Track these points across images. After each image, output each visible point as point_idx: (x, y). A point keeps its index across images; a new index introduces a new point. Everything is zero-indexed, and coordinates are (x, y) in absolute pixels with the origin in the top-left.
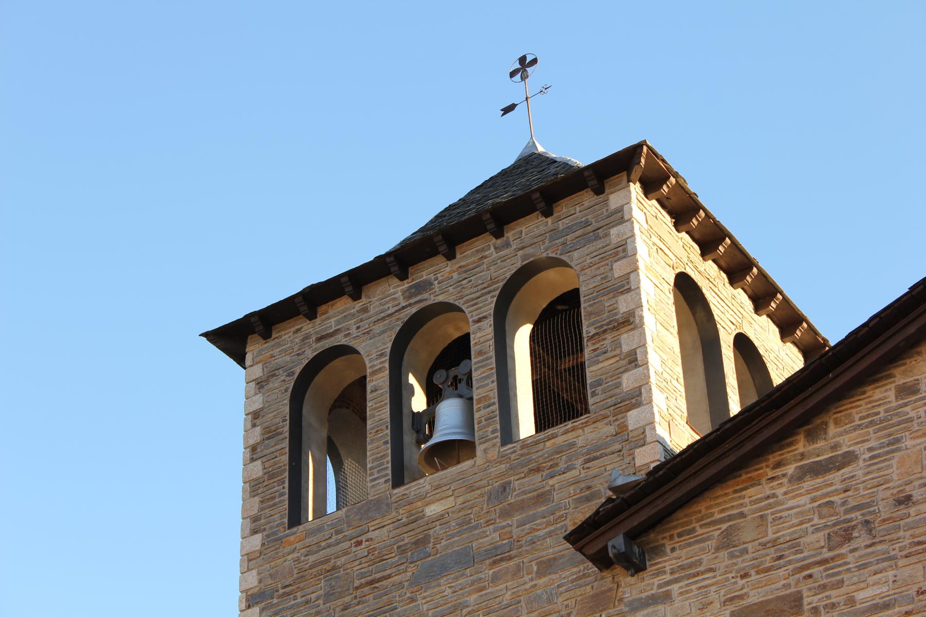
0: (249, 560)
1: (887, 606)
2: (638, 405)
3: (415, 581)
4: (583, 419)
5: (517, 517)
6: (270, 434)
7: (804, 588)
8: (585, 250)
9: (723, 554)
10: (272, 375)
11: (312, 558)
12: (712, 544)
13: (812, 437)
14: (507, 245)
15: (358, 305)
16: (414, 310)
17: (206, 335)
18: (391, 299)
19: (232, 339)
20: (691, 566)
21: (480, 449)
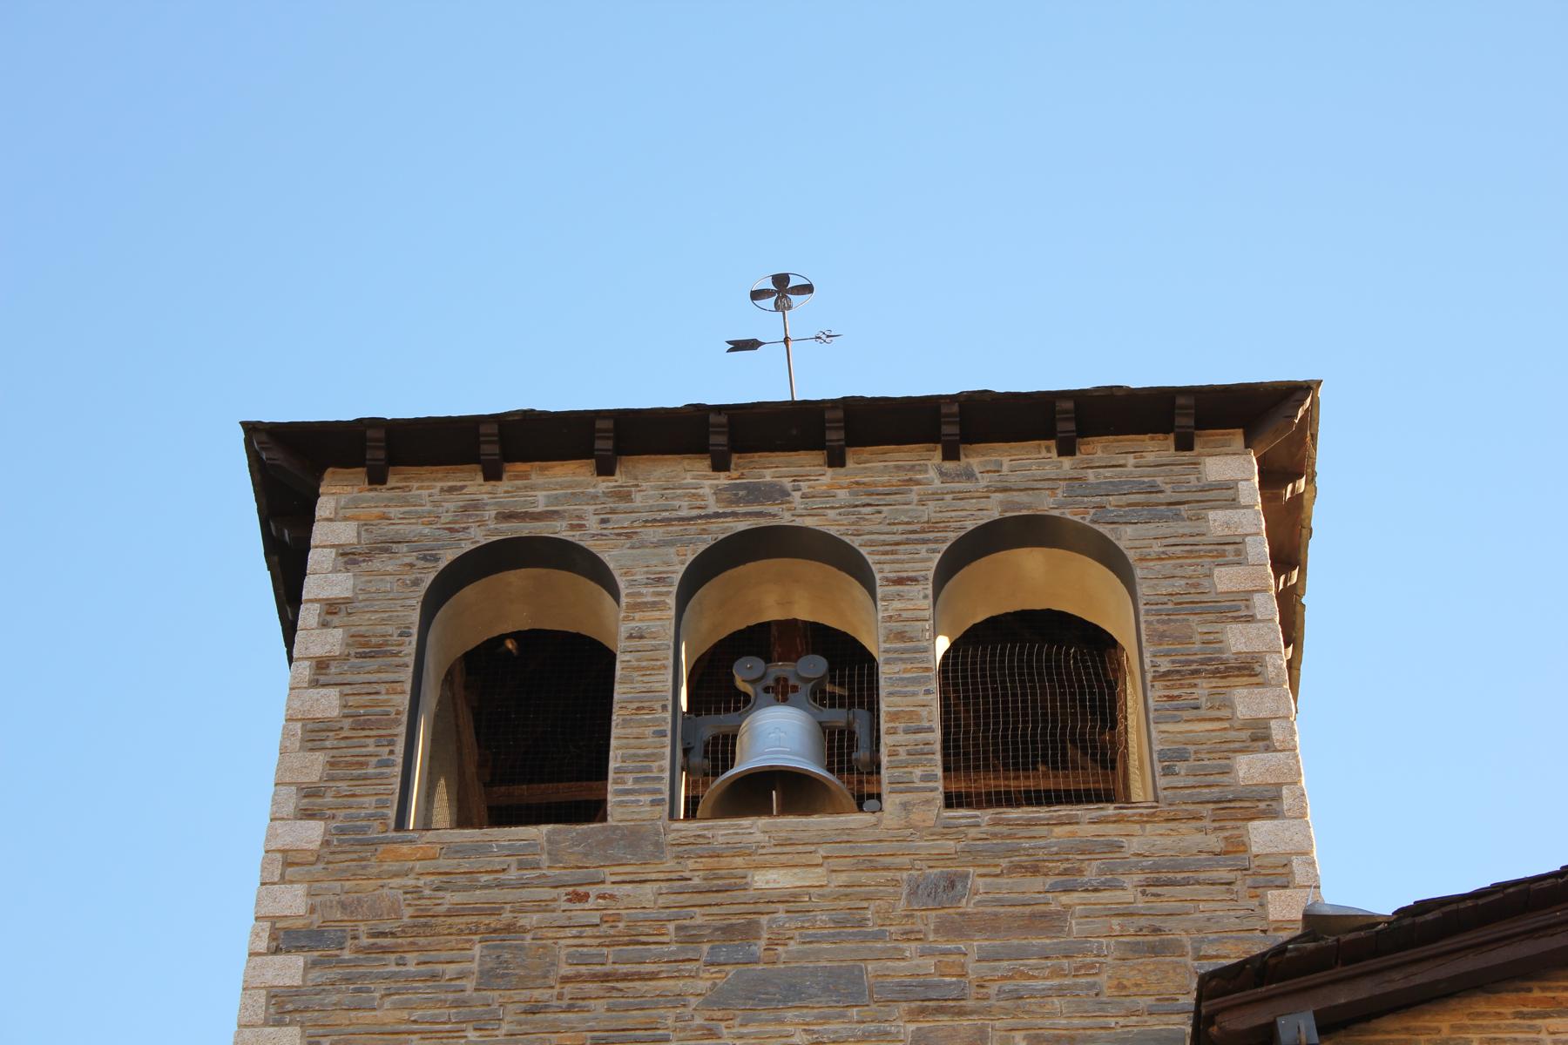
0: (286, 864)
3: (717, 1000)
5: (978, 943)
8: (1152, 529)
11: (451, 898)
15: (604, 485)
16: (742, 526)
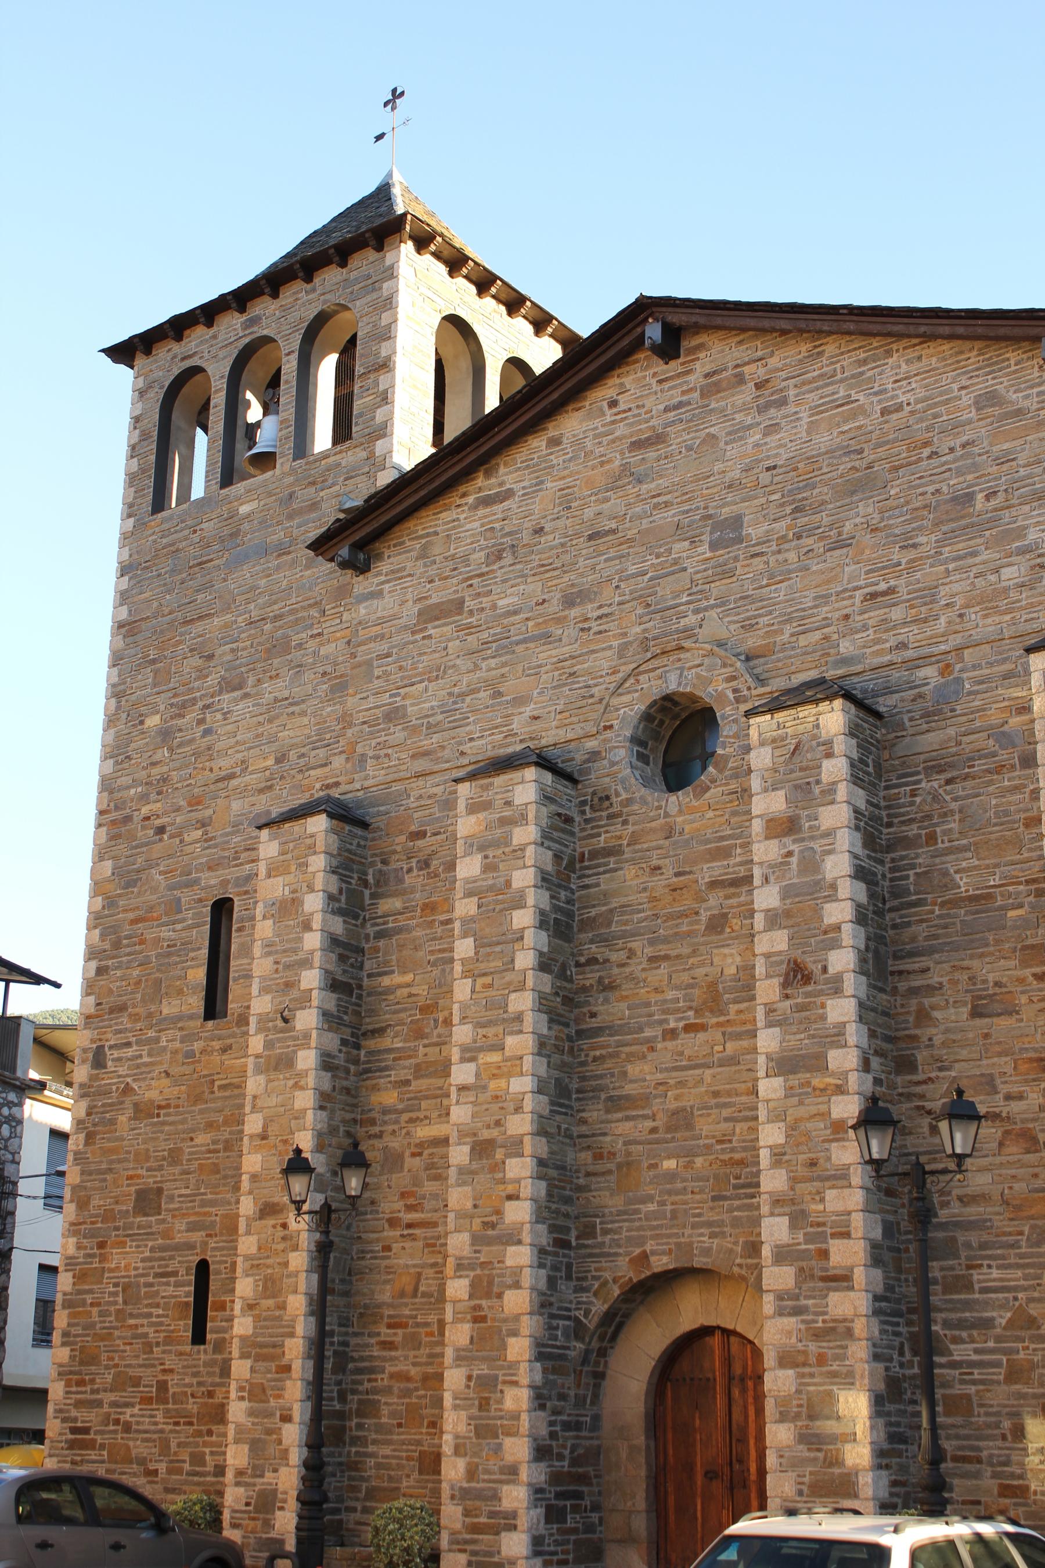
0: (126, 538)
1: (515, 613)
2: (384, 436)
4: (348, 444)
6: (144, 436)
7: (467, 594)
8: (364, 301)
9: (420, 563)
10: (149, 387)
12: (414, 554)
13: (488, 474)
14: (314, 290)
15: (211, 332)
16: (247, 340)
17: (103, 351)
18: (232, 328)
19: (122, 353)
20: (398, 571)
21: (279, 462)
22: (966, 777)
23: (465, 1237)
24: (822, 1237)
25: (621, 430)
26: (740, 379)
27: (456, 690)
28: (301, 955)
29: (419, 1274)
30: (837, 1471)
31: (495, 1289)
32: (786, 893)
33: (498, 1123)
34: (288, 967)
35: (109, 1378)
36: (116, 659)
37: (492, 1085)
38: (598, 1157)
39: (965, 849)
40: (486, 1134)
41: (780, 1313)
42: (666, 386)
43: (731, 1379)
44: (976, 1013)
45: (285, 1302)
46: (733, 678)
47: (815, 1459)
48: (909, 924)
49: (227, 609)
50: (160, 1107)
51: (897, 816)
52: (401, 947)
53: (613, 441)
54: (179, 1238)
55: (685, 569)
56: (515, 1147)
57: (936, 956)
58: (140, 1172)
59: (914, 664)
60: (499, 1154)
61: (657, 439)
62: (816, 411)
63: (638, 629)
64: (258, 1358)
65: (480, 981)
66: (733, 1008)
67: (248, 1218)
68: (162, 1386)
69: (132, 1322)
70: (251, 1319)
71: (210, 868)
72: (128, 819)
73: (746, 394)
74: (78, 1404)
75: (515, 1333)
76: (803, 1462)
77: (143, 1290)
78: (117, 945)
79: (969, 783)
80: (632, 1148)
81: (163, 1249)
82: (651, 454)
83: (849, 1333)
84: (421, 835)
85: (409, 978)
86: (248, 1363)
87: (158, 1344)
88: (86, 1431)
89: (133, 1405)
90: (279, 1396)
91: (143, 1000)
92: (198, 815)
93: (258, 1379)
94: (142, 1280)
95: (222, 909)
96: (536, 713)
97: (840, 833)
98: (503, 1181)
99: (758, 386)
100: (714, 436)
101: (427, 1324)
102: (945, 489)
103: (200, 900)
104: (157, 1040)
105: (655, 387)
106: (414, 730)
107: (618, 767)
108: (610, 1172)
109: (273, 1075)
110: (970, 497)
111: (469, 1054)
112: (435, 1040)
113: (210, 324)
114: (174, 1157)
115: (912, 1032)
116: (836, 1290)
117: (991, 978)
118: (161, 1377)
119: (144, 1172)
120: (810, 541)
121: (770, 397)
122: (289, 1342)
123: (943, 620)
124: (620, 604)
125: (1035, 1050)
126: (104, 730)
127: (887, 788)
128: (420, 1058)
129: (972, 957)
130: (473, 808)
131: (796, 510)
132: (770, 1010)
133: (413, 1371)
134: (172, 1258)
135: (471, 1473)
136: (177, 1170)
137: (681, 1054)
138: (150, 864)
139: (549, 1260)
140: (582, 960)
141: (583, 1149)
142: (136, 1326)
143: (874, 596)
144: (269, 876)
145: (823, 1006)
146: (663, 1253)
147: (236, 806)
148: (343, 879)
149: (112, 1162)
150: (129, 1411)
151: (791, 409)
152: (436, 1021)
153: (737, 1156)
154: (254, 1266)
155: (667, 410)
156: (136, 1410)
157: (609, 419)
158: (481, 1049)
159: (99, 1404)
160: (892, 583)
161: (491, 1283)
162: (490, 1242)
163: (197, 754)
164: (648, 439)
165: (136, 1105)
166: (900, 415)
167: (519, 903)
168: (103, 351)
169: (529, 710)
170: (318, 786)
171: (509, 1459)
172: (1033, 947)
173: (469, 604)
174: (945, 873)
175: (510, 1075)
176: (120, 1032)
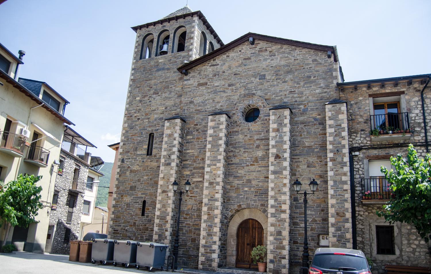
0: (133, 63)
1: (218, 86)
2: (191, 51)
3: (156, 71)
4: (183, 51)
5: (172, 64)
6: (139, 45)
7: (208, 82)
9: (199, 75)
10: (140, 36)
11: (142, 65)
12: (197, 73)
13: (214, 60)
14: (178, 22)
15: (155, 27)
16: (162, 30)
17: (132, 28)
18: (159, 27)
19: (135, 29)
20: (194, 76)
21: (168, 53)
22: (308, 125)
23: (207, 200)
24: (281, 204)
25: (241, 56)
26: (266, 50)
27: (205, 99)
28: (173, 145)
29: (193, 206)
30: (281, 245)
31: (213, 209)
32: (276, 142)
33: (215, 179)
34: (170, 147)
35: (123, 221)
36: (130, 86)
37: (214, 172)
38: (231, 187)
39: (308, 138)
40: (212, 181)
41: (272, 217)
42: (251, 49)
43: (253, 228)
44: (308, 167)
45: (167, 209)
46: (263, 103)
47: (277, 243)
48: (296, 150)
49: (155, 79)
50: (136, 171)
51: (295, 131)
52: (192, 145)
53: (240, 58)
54: (139, 196)
55: (253, 83)
56: (218, 184)
57: (301, 156)
58: (131, 183)
59: (299, 105)
60: (215, 185)
61: (249, 59)
62: (281, 58)
63: (244, 92)
64: (161, 219)
65: (212, 153)
66: (260, 162)
67: (159, 193)
68: (135, 223)
69: (128, 211)
70: (159, 212)
71: (149, 127)
72: (131, 116)
73: (268, 53)
74: (116, 225)
75: (216, 218)
76: (275, 243)
77: (131, 205)
78: (128, 140)
79: (309, 127)
80: (238, 185)
81: (135, 197)
82: (247, 61)
83: (285, 221)
84: (197, 125)
85: (193, 151)
86: (159, 220)
87: (134, 215)
88: (117, 231)
89: (128, 226)
90: (165, 227)
91: (133, 151)
92: (148, 117)
93: (161, 223)
94: (131, 203)
95: (151, 136)
96: (222, 105)
97: (287, 133)
98: (215, 190)
99: (270, 52)
100: (261, 60)
101: (194, 215)
102: (306, 75)
103: (147, 133)
104: (136, 158)
105: (249, 49)
106: (196, 106)
107: (239, 117)
108: (234, 190)
109: (166, 166)
110: (310, 77)
111: (209, 166)
112: (198, 163)
113: (154, 26)
114: (139, 180)
115: (296, 169)
116: (283, 213)
117: (311, 161)
118: (134, 222)
119: (132, 183)
120: (279, 81)
121: (272, 54)
122: (167, 217)
123: (304, 98)
124: (240, 87)
125: (319, 174)
126: (127, 99)
127: (293, 126)
128: (195, 166)
129: (307, 157)
130: (212, 121)
131: (277, 75)
132: (272, 163)
133: (191, 223)
134: (137, 199)
135: (206, 242)
136: (139, 183)
137: (249, 169)
138: (136, 125)
139: (223, 205)
140: (230, 151)
141: (228, 185)
142: (129, 212)
143: (291, 92)
144: (167, 129)
145: (283, 163)
146: (244, 205)
147: (156, 116)
148: (182, 131)
149: (125, 180)
150: (127, 227)
151: (276, 57)
152: (198, 159)
153: (260, 188)
154: (161, 202)
155: (251, 54)
156: (129, 227)
157: (239, 54)
158: (212, 165)
159: (121, 226)
160: (295, 90)
161: (212, 208)
162: (212, 200)
163: (147, 105)
164: (247, 58)
165: (131, 170)
166: (298, 61)
167: (221, 139)
168: (132, 28)
169: (220, 104)
170: (174, 114)
171: (214, 240)
172: (319, 156)
173: (208, 84)
174: (303, 142)
175: (217, 170)
176: (128, 156)
